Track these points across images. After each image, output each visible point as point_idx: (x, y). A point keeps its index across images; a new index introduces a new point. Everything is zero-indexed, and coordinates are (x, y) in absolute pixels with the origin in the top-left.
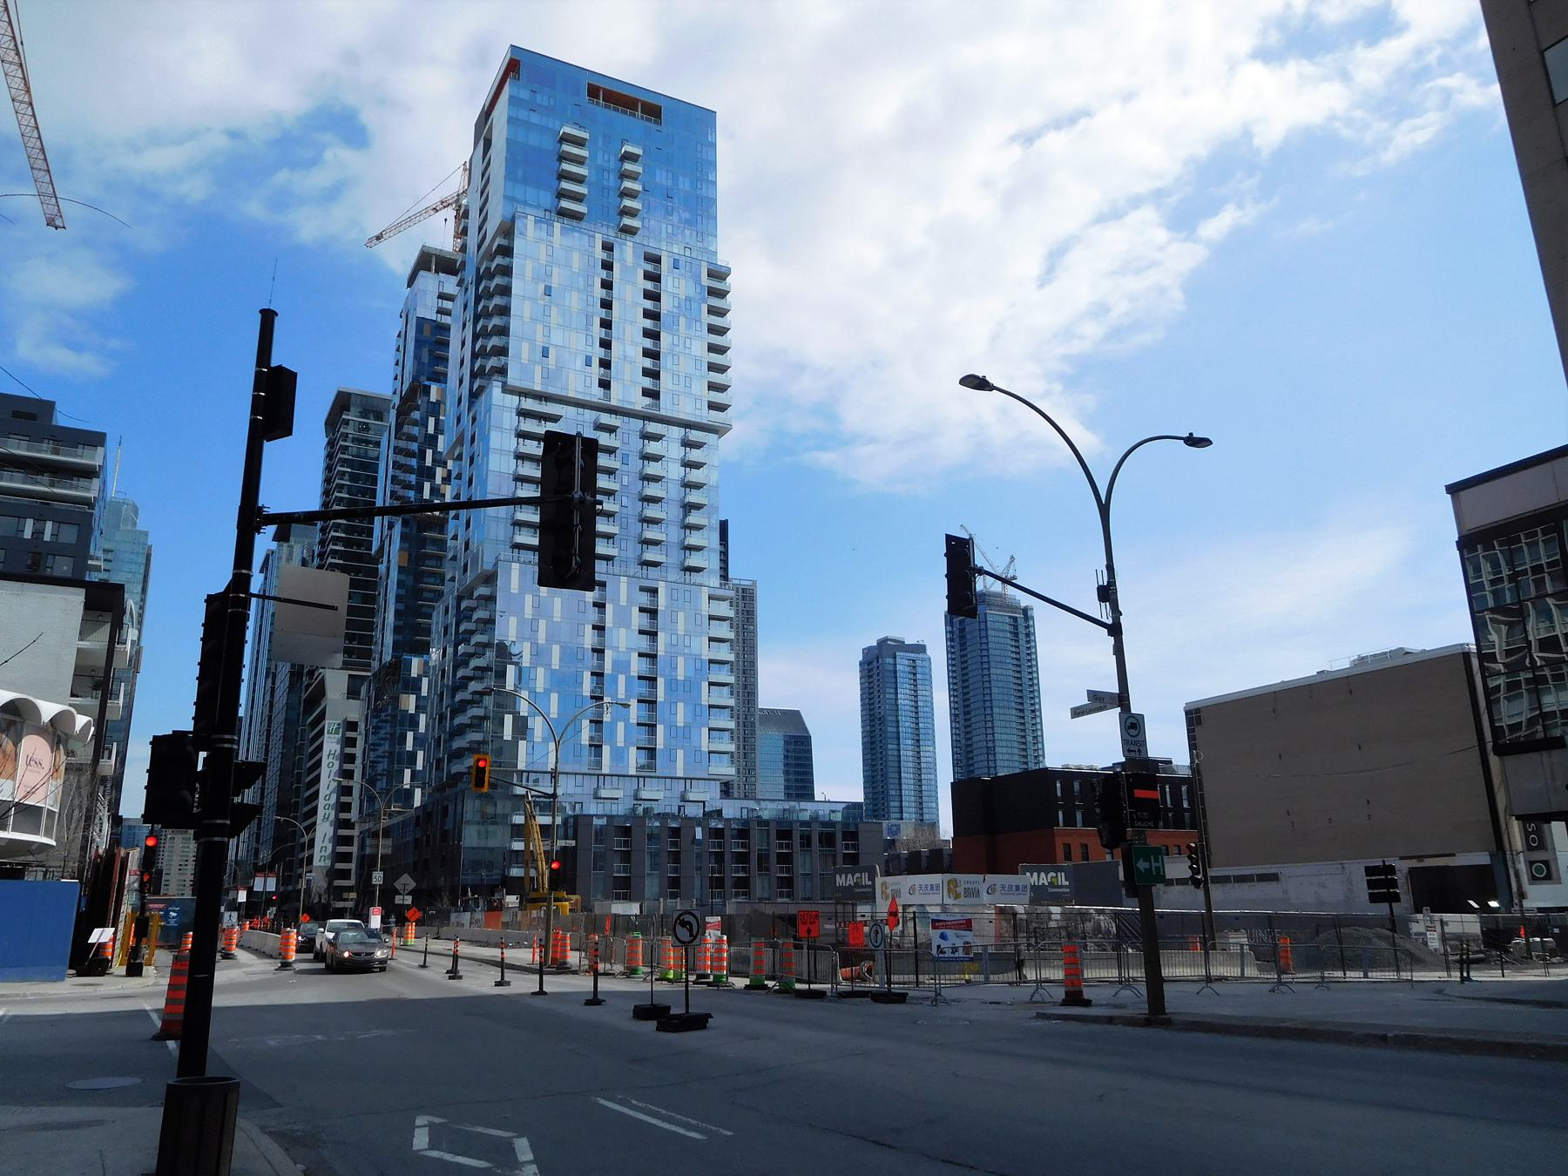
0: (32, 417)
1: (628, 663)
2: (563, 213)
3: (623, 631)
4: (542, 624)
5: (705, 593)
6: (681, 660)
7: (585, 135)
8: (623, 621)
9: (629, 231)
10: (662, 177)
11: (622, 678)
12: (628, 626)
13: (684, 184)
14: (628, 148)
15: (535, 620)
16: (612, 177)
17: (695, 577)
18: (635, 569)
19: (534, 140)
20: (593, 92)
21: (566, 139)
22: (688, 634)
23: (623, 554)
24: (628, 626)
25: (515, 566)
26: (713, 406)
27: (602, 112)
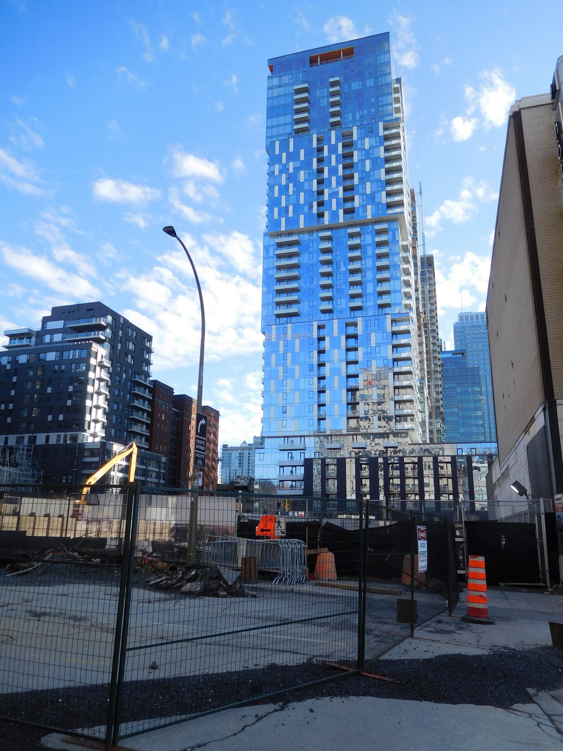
0: (92, 310)
1: (340, 369)
2: (297, 131)
3: (336, 351)
4: (289, 355)
5: (389, 319)
6: (374, 362)
7: (306, 85)
8: (335, 344)
9: (334, 125)
10: (356, 86)
11: (336, 378)
12: (339, 347)
13: (370, 83)
14: (331, 80)
15: (285, 354)
16: (325, 100)
17: (387, 310)
18: (348, 314)
19: (282, 101)
20: (313, 61)
21: (298, 92)
22: (378, 345)
23: (339, 307)
24: (339, 347)
25: (274, 327)
26: (390, 206)
27: (320, 67)
